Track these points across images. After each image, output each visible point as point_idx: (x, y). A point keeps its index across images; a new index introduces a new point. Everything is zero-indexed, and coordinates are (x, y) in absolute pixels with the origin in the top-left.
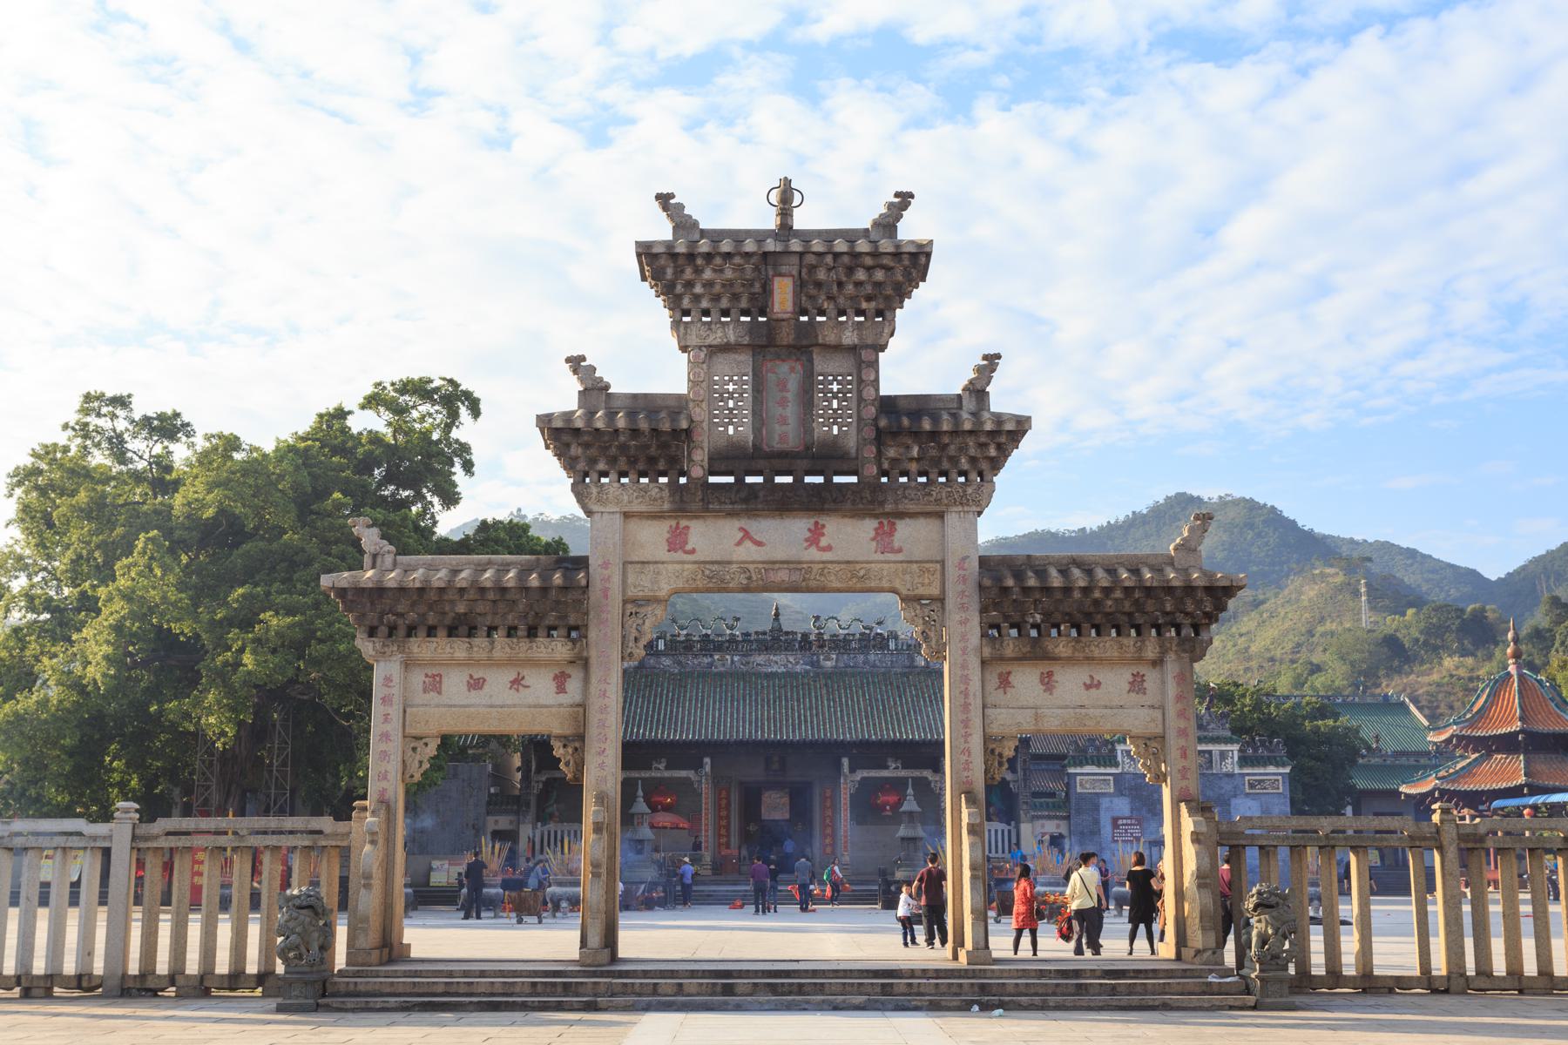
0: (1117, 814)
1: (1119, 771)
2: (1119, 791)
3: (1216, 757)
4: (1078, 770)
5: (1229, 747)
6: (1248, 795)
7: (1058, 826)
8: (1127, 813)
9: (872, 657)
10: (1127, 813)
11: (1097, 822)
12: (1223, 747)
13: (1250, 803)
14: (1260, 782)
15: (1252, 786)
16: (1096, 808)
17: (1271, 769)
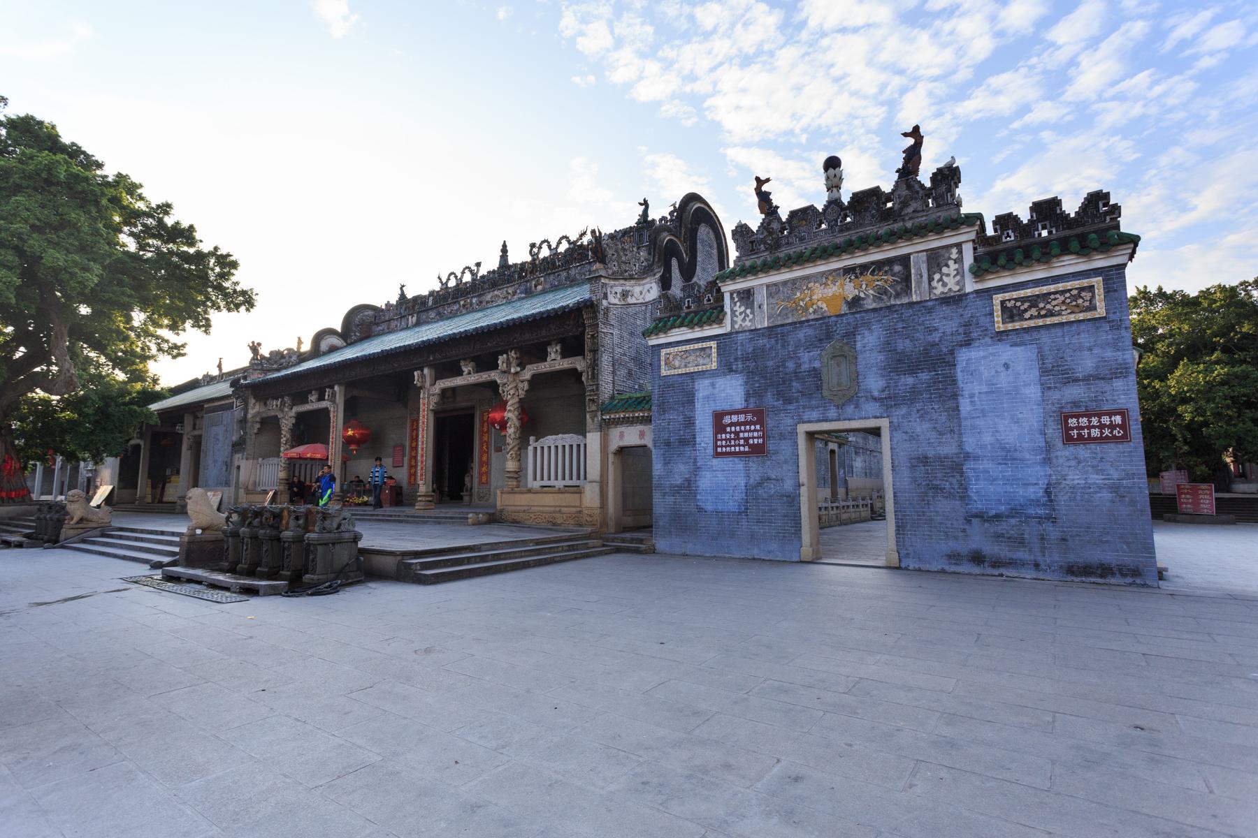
0: (721, 406)
1: (726, 328)
2: (727, 367)
3: (919, 265)
4: (662, 339)
5: (949, 239)
6: (1001, 336)
7: (642, 434)
8: (739, 403)
9: (573, 272)
10: (739, 403)
11: (690, 423)
12: (934, 242)
13: (1006, 352)
14: (1033, 301)
15: (1010, 313)
16: (690, 399)
17: (1069, 264)
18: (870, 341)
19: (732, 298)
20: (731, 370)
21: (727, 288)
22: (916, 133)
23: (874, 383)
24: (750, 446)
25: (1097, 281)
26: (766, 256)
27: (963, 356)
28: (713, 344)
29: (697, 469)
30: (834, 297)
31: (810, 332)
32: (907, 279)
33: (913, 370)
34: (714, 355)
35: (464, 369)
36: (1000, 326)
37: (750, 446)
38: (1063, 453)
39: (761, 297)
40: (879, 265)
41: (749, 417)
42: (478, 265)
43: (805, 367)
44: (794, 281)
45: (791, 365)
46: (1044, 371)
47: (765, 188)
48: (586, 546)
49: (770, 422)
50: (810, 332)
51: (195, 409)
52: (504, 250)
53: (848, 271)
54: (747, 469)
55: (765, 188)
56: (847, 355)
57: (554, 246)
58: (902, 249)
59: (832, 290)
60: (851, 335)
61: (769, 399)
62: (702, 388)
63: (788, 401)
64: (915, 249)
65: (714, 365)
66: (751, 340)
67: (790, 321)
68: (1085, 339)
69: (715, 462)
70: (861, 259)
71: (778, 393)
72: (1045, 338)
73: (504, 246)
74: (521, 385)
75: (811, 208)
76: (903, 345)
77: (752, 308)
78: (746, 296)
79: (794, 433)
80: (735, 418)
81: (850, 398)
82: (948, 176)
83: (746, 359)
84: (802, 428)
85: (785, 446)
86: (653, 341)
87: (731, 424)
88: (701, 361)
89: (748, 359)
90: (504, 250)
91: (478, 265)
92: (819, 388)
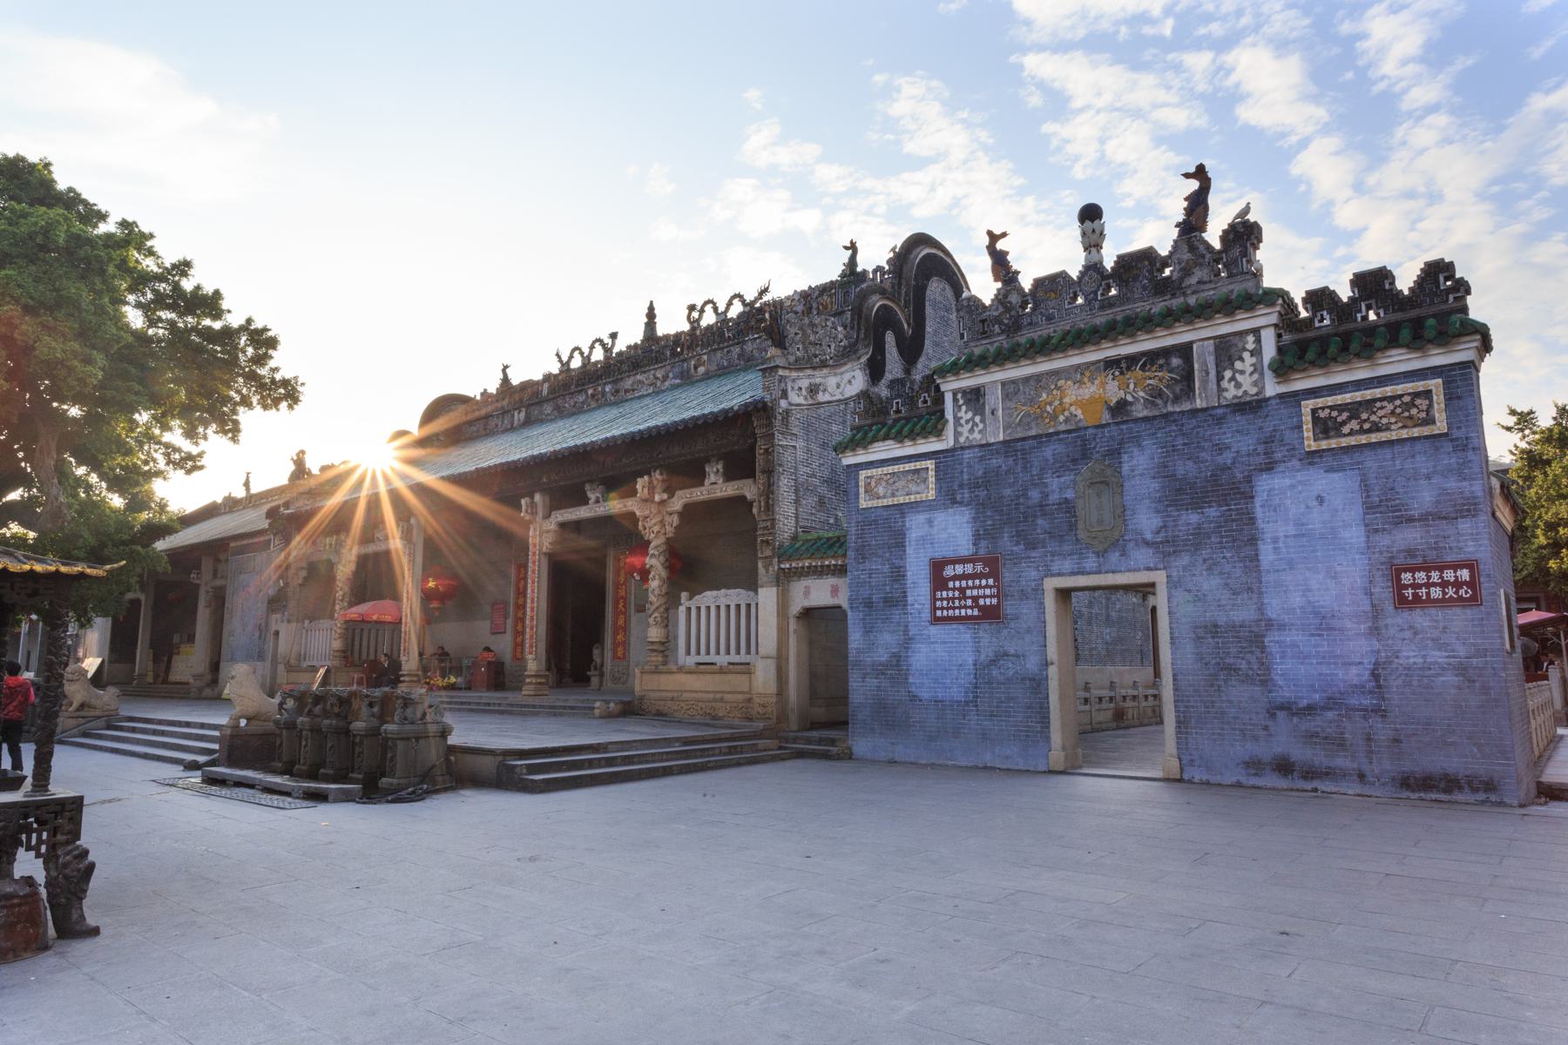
2: (949, 497)
3: (1204, 358)
4: (861, 457)
5: (1242, 323)
6: (1313, 457)
7: (835, 591)
8: (964, 546)
9: (749, 347)
10: (964, 546)
11: (898, 574)
13: (1320, 481)
14: (1354, 410)
15: (1325, 427)
16: (898, 541)
17: (1398, 361)
18: (1139, 462)
19: (955, 400)
20: (954, 502)
21: (949, 386)
22: (1200, 173)
23: (1146, 521)
24: (981, 608)
25: (1435, 384)
26: (1001, 341)
27: (1265, 485)
28: (930, 464)
29: (907, 642)
30: (1092, 400)
31: (1061, 448)
32: (1188, 376)
33: (1197, 504)
34: (932, 479)
35: (590, 494)
36: (1311, 444)
37: (981, 608)
38: (1395, 620)
39: (994, 399)
40: (1152, 357)
41: (979, 568)
42: (614, 336)
43: (1054, 498)
44: (1038, 378)
45: (1035, 495)
46: (1369, 507)
47: (1000, 245)
48: (754, 748)
49: (1007, 575)
50: (1061, 448)
51: (217, 549)
52: (651, 314)
53: (1110, 364)
54: (976, 640)
55: (1000, 245)
56: (1110, 482)
57: (721, 309)
58: (1181, 335)
59: (1089, 390)
60: (1115, 453)
61: (1006, 543)
62: (916, 525)
63: (1031, 545)
64: (1200, 335)
65: (931, 495)
66: (982, 459)
67: (1033, 433)
68: (1422, 463)
69: (934, 630)
70: (1126, 348)
71: (1019, 534)
72: (1371, 462)
73: (651, 309)
74: (668, 519)
75: (1063, 275)
76: (1184, 468)
77: (982, 414)
78: (975, 397)
79: (1039, 590)
80: (959, 569)
81: (1114, 542)
82: (1244, 234)
83: (974, 486)
84: (1051, 584)
85: (1027, 610)
86: (849, 459)
87: (955, 578)
88: (914, 488)
89: (977, 486)
90: (651, 314)
91: (614, 336)
92: (1073, 527)
